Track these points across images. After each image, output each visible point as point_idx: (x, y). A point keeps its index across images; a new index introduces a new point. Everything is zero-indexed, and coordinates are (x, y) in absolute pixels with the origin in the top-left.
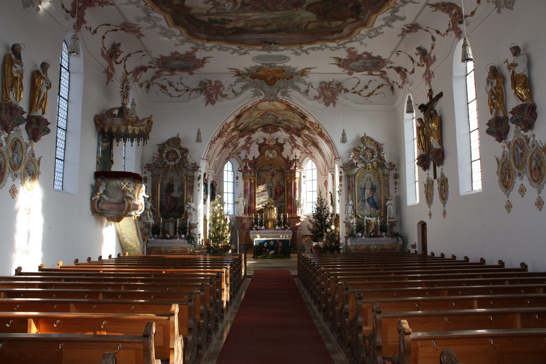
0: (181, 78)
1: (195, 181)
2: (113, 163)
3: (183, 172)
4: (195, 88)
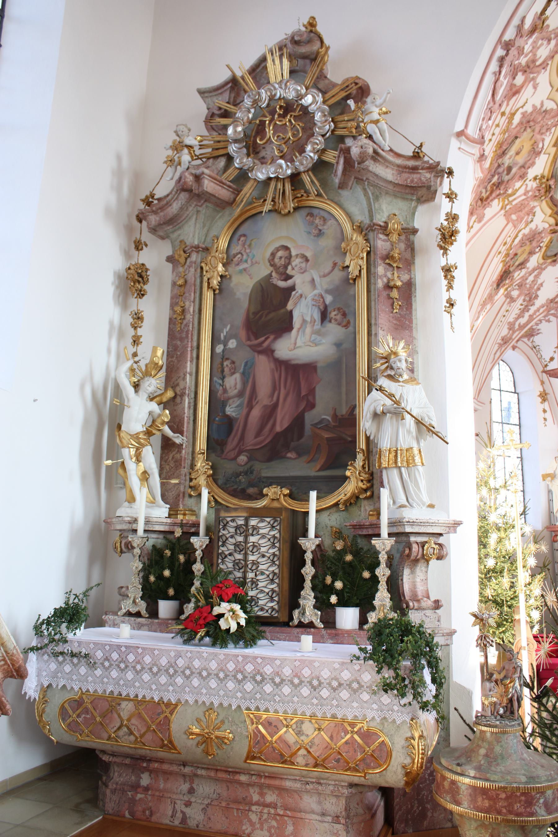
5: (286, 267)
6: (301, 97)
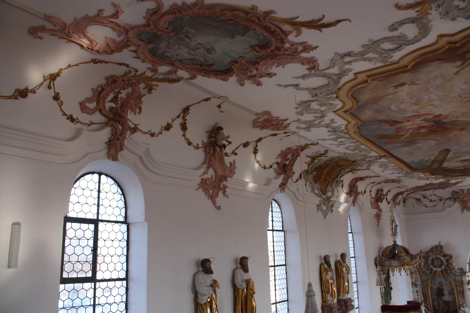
0: (434, 191)
1: (464, 285)
2: (391, 289)
3: (451, 278)
4: (448, 197)
5: (442, 285)
6: (440, 257)
